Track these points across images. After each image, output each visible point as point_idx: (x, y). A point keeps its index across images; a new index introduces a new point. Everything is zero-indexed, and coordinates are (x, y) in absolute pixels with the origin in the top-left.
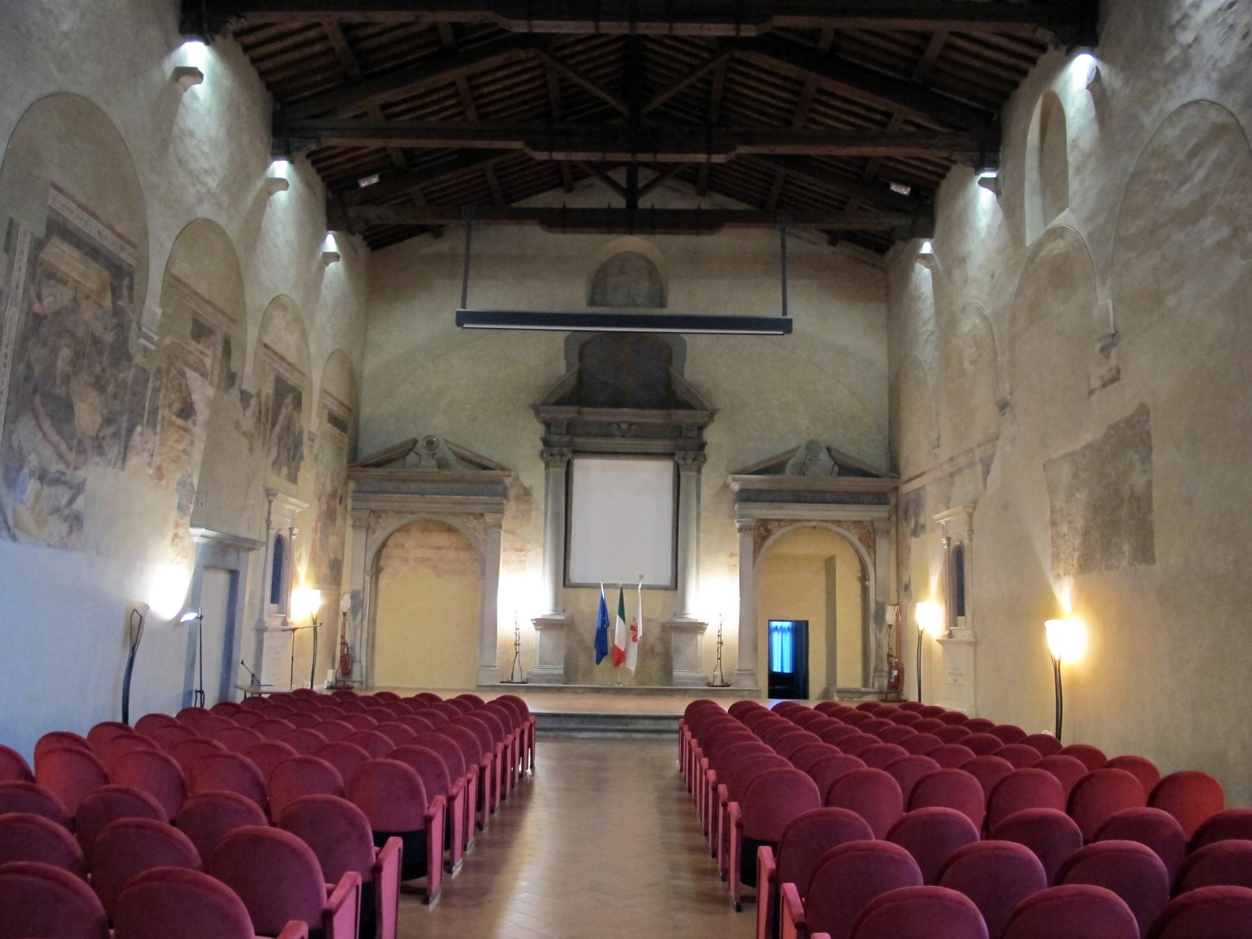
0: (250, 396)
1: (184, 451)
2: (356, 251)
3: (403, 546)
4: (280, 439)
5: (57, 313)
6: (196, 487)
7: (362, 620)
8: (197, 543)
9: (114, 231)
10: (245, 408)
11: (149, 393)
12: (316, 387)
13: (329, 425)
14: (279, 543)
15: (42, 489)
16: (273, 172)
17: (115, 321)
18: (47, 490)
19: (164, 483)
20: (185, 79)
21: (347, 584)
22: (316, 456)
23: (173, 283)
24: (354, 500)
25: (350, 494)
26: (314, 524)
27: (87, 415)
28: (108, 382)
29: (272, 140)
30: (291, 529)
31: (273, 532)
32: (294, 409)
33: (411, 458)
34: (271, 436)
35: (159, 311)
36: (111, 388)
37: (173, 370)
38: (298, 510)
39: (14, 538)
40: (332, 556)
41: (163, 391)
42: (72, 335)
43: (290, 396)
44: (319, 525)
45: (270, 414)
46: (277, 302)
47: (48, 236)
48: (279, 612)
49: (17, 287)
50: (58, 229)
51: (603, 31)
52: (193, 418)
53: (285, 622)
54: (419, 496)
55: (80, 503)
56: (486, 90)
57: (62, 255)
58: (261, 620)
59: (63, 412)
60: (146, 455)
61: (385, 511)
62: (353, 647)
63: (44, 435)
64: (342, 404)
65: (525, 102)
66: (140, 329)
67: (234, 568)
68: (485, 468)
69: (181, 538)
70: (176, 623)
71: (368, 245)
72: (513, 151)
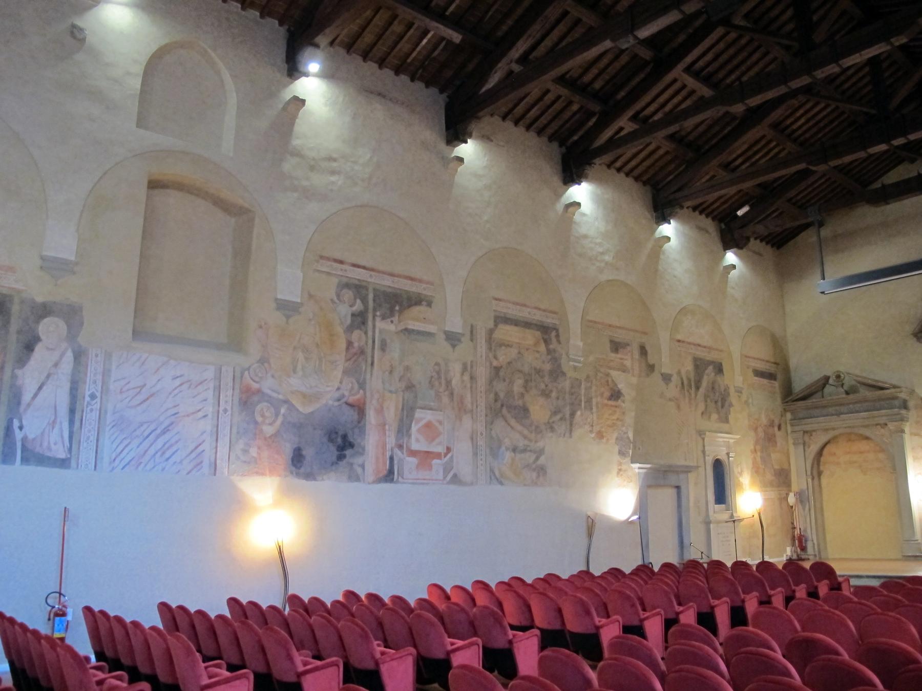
0: (671, 375)
1: (618, 419)
2: (760, 255)
3: (835, 454)
4: (706, 397)
5: (509, 363)
6: (631, 438)
7: (810, 510)
8: (639, 473)
9: (540, 309)
10: (667, 384)
11: (583, 392)
12: (736, 355)
13: (756, 378)
14: (718, 466)
15: (515, 456)
16: (661, 232)
17: (549, 357)
18: (518, 456)
19: (604, 440)
20: (571, 210)
21: (795, 487)
22: (746, 402)
23: (589, 325)
24: (792, 425)
25: (788, 422)
26: (752, 447)
27: (539, 410)
28: (551, 391)
29: (654, 214)
30: (728, 454)
31: (710, 460)
32: (715, 375)
33: (828, 389)
34: (696, 395)
35: (581, 344)
36: (554, 394)
37: (598, 374)
38: (732, 441)
39: (501, 483)
40: (777, 467)
41: (594, 388)
42: (520, 371)
43: (711, 368)
44: (758, 447)
45: (693, 384)
46: (684, 311)
47: (496, 325)
48: (727, 509)
49: (481, 356)
50: (502, 319)
51: (845, 66)
52: (622, 398)
53: (732, 516)
54: (836, 416)
55: (542, 460)
56: (795, 127)
57: (507, 332)
58: (707, 515)
59: (523, 413)
60: (587, 428)
61: (814, 431)
62: (805, 530)
63: (512, 428)
64: (768, 361)
65: (832, 122)
66: (568, 357)
67: (677, 485)
68: (882, 389)
69: (625, 471)
70: (628, 523)
71: (772, 246)
72: (779, 178)
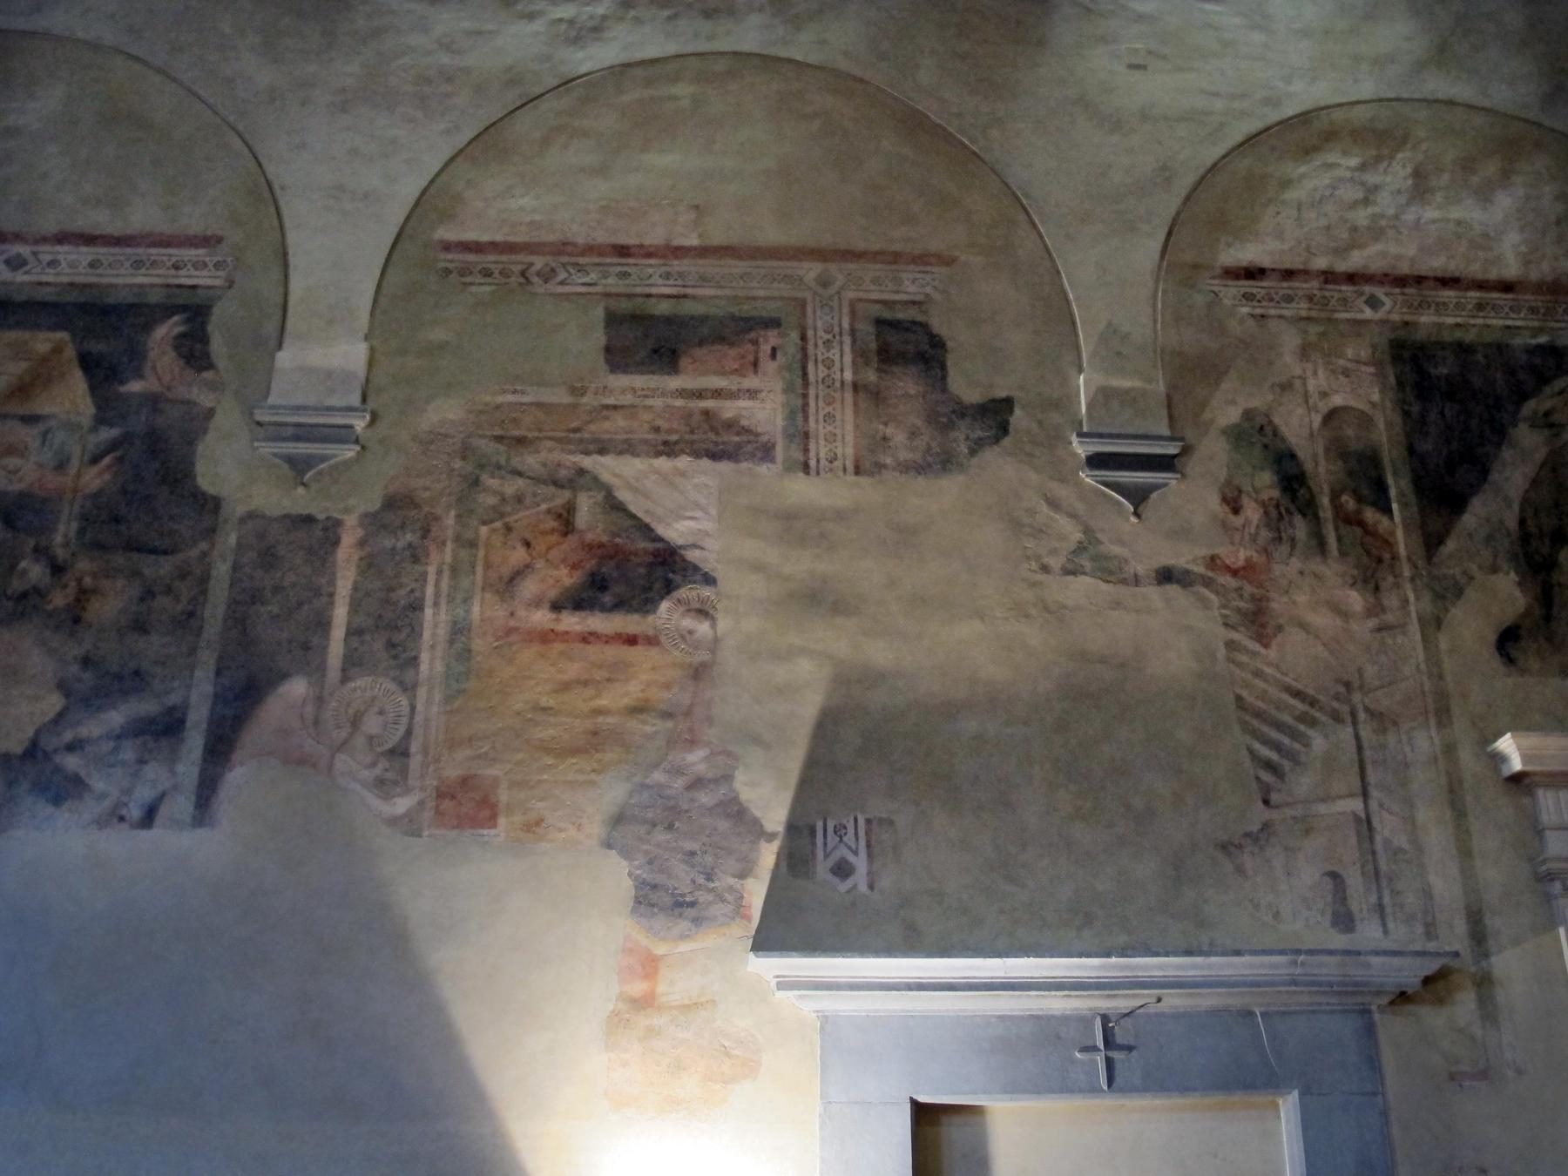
1: (637, 710)
